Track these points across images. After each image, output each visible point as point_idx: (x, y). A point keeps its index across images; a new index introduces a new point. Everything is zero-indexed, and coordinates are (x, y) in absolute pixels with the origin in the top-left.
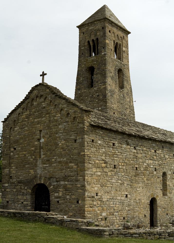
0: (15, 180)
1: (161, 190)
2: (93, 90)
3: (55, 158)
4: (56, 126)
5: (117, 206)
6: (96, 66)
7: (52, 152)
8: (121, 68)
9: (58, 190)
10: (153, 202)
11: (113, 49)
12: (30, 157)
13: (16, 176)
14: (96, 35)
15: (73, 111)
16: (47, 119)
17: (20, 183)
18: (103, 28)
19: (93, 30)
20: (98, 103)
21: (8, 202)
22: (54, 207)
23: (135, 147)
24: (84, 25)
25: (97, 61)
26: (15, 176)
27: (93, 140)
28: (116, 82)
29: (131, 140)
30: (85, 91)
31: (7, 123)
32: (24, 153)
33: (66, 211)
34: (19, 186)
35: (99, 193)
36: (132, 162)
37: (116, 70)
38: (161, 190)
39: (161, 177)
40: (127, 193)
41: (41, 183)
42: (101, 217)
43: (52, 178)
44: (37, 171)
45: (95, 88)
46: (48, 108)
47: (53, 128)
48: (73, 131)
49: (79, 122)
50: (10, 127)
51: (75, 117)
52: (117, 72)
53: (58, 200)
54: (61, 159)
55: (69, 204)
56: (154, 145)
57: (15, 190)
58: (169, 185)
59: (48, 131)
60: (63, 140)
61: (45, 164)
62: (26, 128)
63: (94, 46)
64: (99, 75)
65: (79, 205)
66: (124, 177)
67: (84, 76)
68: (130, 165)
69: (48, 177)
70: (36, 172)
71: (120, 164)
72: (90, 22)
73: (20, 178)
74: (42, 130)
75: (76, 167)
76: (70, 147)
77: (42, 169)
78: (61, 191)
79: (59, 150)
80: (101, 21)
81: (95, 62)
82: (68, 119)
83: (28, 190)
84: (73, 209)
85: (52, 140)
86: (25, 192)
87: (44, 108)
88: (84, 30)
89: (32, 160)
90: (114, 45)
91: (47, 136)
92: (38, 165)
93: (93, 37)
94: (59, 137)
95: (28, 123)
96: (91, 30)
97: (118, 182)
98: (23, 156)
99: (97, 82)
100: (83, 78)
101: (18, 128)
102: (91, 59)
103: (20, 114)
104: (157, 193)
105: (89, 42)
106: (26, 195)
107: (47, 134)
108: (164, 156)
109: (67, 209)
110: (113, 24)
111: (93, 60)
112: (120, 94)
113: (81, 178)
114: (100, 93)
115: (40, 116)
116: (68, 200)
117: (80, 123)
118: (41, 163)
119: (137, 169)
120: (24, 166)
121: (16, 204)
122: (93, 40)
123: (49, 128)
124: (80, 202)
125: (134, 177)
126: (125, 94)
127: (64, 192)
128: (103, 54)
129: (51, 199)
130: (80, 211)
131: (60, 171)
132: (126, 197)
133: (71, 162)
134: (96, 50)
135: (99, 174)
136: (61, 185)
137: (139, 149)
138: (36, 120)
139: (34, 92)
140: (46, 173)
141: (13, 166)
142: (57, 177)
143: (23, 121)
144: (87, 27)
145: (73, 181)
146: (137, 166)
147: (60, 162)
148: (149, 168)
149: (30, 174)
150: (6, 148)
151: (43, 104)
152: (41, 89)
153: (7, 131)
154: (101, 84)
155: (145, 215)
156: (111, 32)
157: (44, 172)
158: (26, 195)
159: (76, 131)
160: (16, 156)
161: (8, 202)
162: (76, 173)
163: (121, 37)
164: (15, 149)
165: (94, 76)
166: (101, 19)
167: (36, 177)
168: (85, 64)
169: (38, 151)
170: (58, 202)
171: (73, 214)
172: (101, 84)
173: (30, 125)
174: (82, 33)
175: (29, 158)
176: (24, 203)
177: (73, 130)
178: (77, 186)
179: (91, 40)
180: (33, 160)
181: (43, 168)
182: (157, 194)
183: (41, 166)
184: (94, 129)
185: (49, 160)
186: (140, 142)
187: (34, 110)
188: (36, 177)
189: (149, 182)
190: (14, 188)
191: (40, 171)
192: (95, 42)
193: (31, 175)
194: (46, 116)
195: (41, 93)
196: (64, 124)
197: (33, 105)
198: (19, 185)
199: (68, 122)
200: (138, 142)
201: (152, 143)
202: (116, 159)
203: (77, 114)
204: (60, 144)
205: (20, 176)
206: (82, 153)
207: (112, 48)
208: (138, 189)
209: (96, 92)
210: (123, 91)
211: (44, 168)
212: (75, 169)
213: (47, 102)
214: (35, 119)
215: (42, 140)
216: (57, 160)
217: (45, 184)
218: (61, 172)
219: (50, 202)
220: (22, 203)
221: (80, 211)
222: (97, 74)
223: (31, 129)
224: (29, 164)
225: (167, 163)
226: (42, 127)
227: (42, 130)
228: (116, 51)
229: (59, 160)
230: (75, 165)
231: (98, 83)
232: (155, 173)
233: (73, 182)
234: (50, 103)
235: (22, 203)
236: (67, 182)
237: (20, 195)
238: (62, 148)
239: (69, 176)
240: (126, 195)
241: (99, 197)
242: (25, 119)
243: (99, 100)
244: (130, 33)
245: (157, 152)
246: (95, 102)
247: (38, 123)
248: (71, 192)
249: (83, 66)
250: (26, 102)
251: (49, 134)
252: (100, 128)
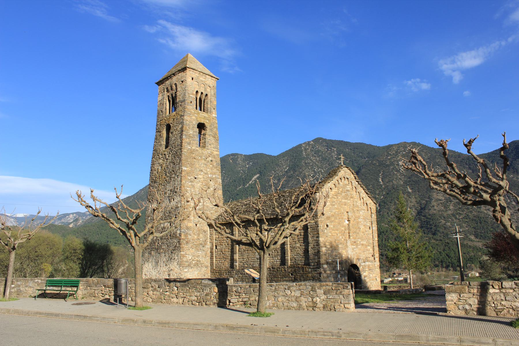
14: (205, 90)
62: (336, 206)
64: (211, 137)
89: (343, 240)
111: (205, 117)
114: (213, 159)
122: (202, 93)
128: (214, 115)
147: (362, 244)
185: (355, 242)
229: (361, 243)
238: (363, 232)
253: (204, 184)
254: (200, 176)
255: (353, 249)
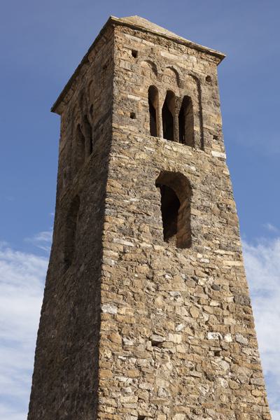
6: (196, 182)
19: (176, 64)
24: (141, 30)
30: (157, 247)
45: (199, 255)
67: (146, 191)
80: (203, 54)
96: (165, 59)
102: (175, 149)
111: (182, 154)
122: (170, 94)
128: (216, 154)
144: (152, 44)
154: (220, 247)
165: (193, 211)
166: (208, 52)
172: (222, 252)
174: (130, 52)
179: (165, 90)
209: (207, 270)
246: (206, 308)
253: (189, 364)
254: (172, 337)
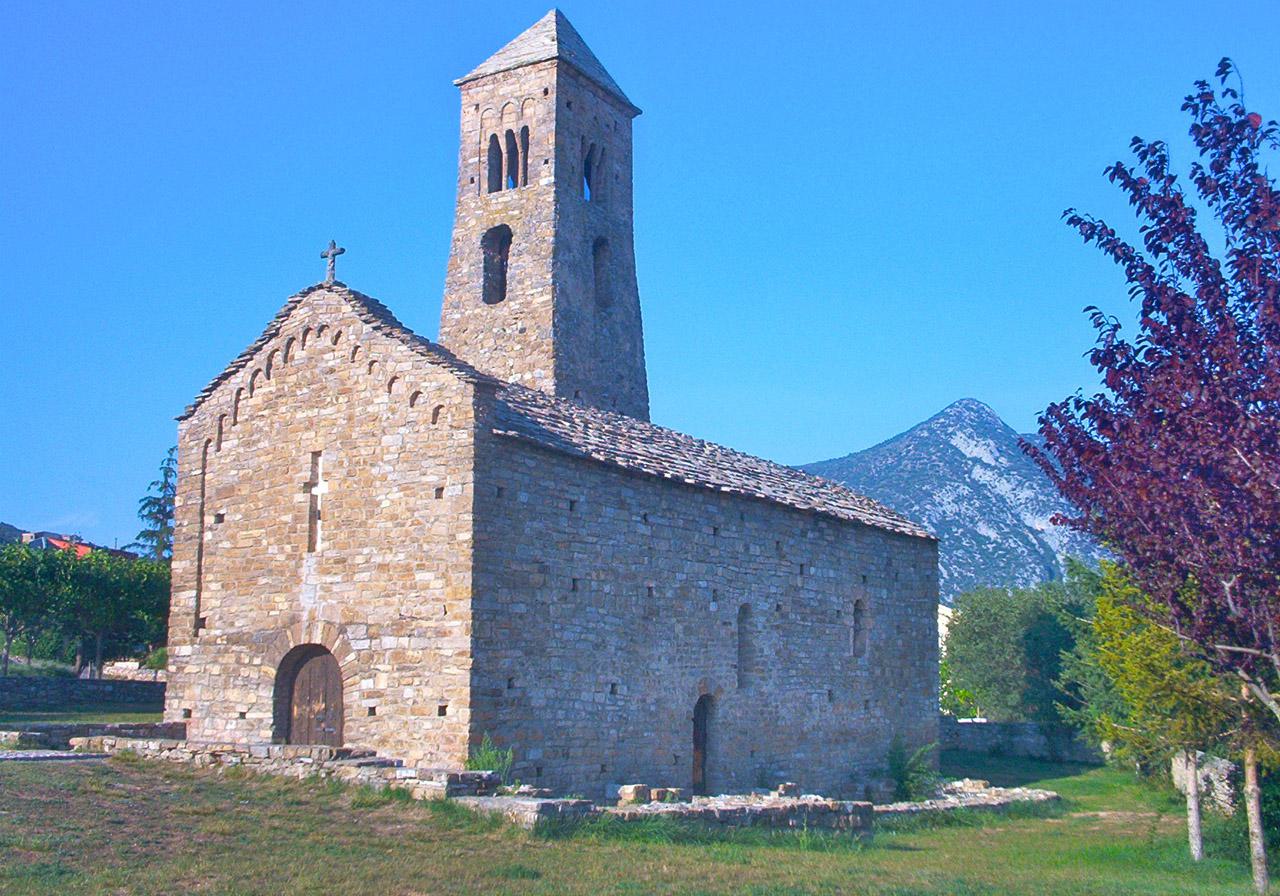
0: (218, 632)
1: (735, 667)
2: (505, 308)
3: (366, 551)
4: (371, 439)
5: (580, 725)
7: (354, 532)
8: (604, 235)
9: (372, 667)
10: (704, 707)
11: (579, 168)
12: (276, 547)
13: (221, 618)
15: (434, 384)
16: (339, 412)
17: (236, 643)
18: (546, 92)
20: (521, 356)
21: (188, 713)
22: (358, 730)
23: (645, 517)
25: (521, 207)
26: (217, 617)
27: (500, 489)
28: (585, 282)
29: (632, 488)
31: (194, 422)
32: (255, 533)
33: (401, 742)
34: (233, 655)
35: (519, 677)
36: (633, 567)
37: (587, 242)
38: (735, 667)
39: (734, 621)
40: (614, 679)
41: (313, 642)
42: (525, 764)
43: (350, 623)
44: (301, 597)
45: (512, 304)
46: (345, 374)
47: (361, 443)
48: (430, 457)
49: (454, 424)
50: (205, 440)
51: (441, 406)
52: (591, 250)
53: (372, 703)
54: (389, 558)
55: (413, 717)
56: (712, 509)
57: (216, 670)
58: (762, 651)
59: (342, 454)
60: (396, 489)
61: (327, 572)
63: (512, 151)
64: (526, 257)
65: (446, 721)
66: (605, 623)
68: (625, 577)
69: (338, 620)
70: (295, 604)
71: (594, 574)
72: (502, 68)
73: (237, 624)
74: (320, 452)
75: (440, 583)
76: (422, 513)
77: (316, 591)
78: (383, 672)
79: (382, 525)
81: (516, 212)
82: (416, 414)
83: (264, 668)
84: (427, 737)
85: (355, 486)
86: (254, 675)
87: (332, 371)
88: (480, 95)
89: (281, 558)
90: (582, 151)
91: (341, 473)
92: (303, 578)
93: (511, 123)
94: (384, 478)
95: (272, 423)
97: (585, 640)
98: (251, 542)
99: (520, 282)
100: (471, 266)
101: (236, 442)
102: (500, 200)
103: (242, 392)
104: (720, 678)
105: (494, 138)
106: (259, 684)
107: (341, 463)
108: (747, 549)
109: (403, 736)
110: (581, 78)
112: (598, 327)
113: (457, 623)
115: (317, 402)
116: (410, 702)
117: (458, 428)
118: (315, 570)
119: (650, 595)
120: (252, 580)
121: (218, 720)
122: (510, 133)
123: (347, 442)
124: (448, 710)
125: (642, 622)
126: (618, 327)
127: (396, 675)
129: (346, 701)
130: (449, 741)
131: (382, 600)
132: (613, 692)
133: (421, 567)
134: (520, 171)
135: (522, 608)
136: (386, 650)
137: (660, 521)
138: (300, 415)
139: (293, 312)
140: (332, 607)
141: (210, 582)
142: (370, 622)
143: (252, 418)
144: (492, 87)
145: (429, 634)
146: (652, 585)
147: (382, 567)
148: (693, 590)
149: (274, 609)
150: (189, 515)
151: (327, 356)
152: (321, 302)
153: (193, 452)
155: (676, 757)
156: (572, 105)
157: (324, 604)
158: (255, 687)
159: (442, 456)
160: (226, 544)
161: (188, 713)
162: (440, 605)
163: (608, 126)
164: (220, 518)
166: (540, 62)
167: (294, 620)
168: (478, 218)
169: (304, 525)
170: (372, 711)
171: (425, 755)
172: (535, 291)
173: (278, 433)
175: (270, 551)
176: (247, 716)
177: (431, 455)
178: (442, 652)
180: (289, 557)
181: (322, 588)
182: (721, 682)
183: (312, 580)
184: (506, 451)
185: (343, 561)
186: (664, 497)
187: (293, 378)
188: (294, 620)
189: (693, 639)
190: (215, 662)
191: (310, 598)
192: (518, 140)
193: (278, 613)
194: (337, 399)
195: (321, 316)
196: (402, 430)
197: (293, 358)
198: (233, 652)
199: (416, 423)
200: (658, 499)
201: (704, 503)
202: (581, 556)
203: (450, 394)
204: (386, 504)
205: (237, 616)
206: (461, 535)
207: (575, 165)
208: (653, 666)
210: (610, 314)
211: (327, 589)
212: (437, 592)
213: (344, 348)
214: (296, 409)
215: (321, 489)
216: (372, 560)
217: (328, 647)
218: (386, 604)
219: (343, 710)
220: (243, 715)
221: (449, 741)
222: (520, 253)
223: (283, 448)
224: (270, 572)
225: (754, 572)
226: (320, 440)
227: (320, 452)
228: (588, 174)
229: (379, 559)
230: (437, 578)
231: (524, 287)
232: (713, 607)
233: (429, 638)
234: (354, 353)
235: (243, 715)
236: (407, 639)
237: (235, 686)
238: (393, 517)
239: (413, 618)
240: (613, 685)
241: (518, 694)
242: (260, 410)
243: (525, 344)
244: (641, 113)
245: (724, 534)
247: (310, 424)
248: (420, 676)
249: (473, 222)
250: (268, 348)
251: (346, 464)
252: (527, 449)
255: (327, 589)
